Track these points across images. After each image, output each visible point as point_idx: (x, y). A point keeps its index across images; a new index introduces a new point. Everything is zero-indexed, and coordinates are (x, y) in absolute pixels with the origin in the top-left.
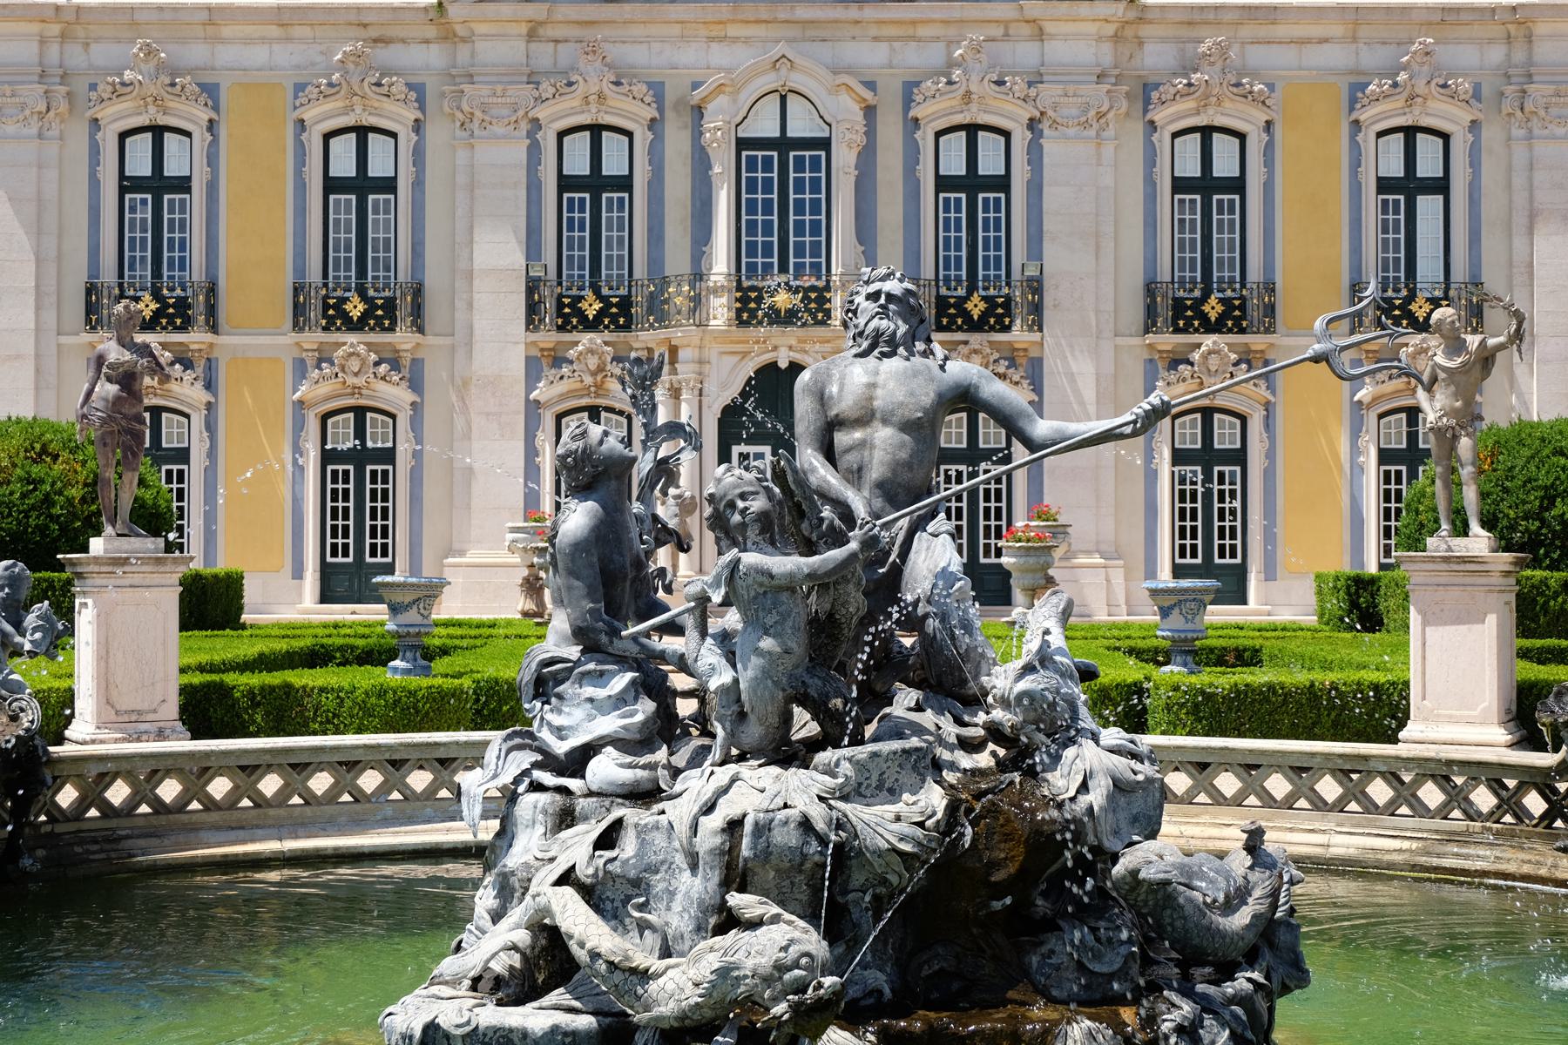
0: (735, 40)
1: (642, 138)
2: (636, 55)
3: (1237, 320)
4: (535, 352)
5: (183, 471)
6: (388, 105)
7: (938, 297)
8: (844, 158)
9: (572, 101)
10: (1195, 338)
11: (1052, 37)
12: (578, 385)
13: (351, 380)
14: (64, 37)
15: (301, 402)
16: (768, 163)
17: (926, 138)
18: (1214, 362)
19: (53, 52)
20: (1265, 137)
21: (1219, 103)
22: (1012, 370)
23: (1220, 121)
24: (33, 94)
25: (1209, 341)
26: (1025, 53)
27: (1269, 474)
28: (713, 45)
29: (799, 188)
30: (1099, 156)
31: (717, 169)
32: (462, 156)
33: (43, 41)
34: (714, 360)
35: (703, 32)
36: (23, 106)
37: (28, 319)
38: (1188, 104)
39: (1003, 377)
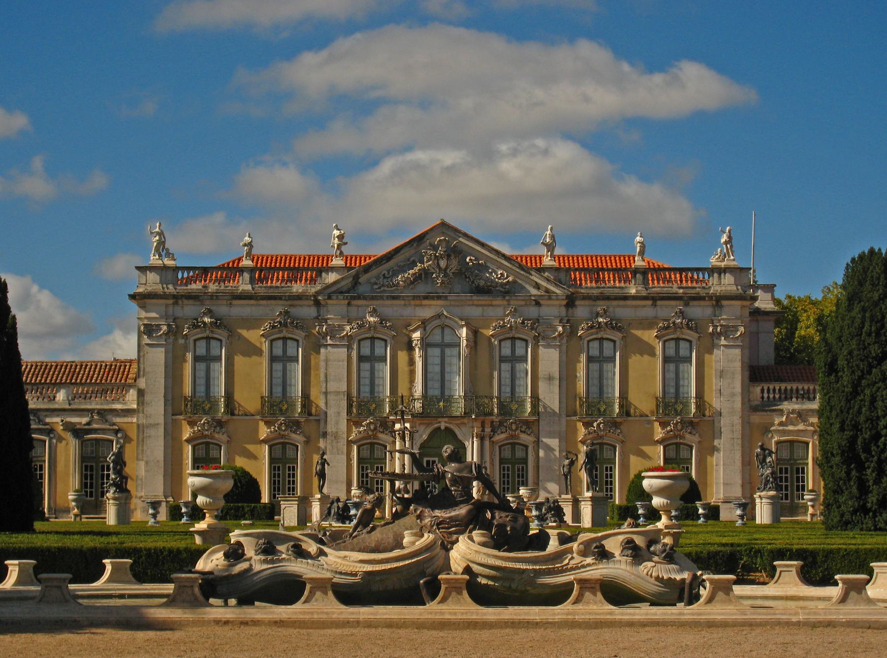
5: (42, 465)
12: (366, 435)
19: (170, 309)
21: (605, 330)
22: (527, 430)
23: (605, 336)
28: (417, 308)
33: (167, 306)
39: (524, 432)
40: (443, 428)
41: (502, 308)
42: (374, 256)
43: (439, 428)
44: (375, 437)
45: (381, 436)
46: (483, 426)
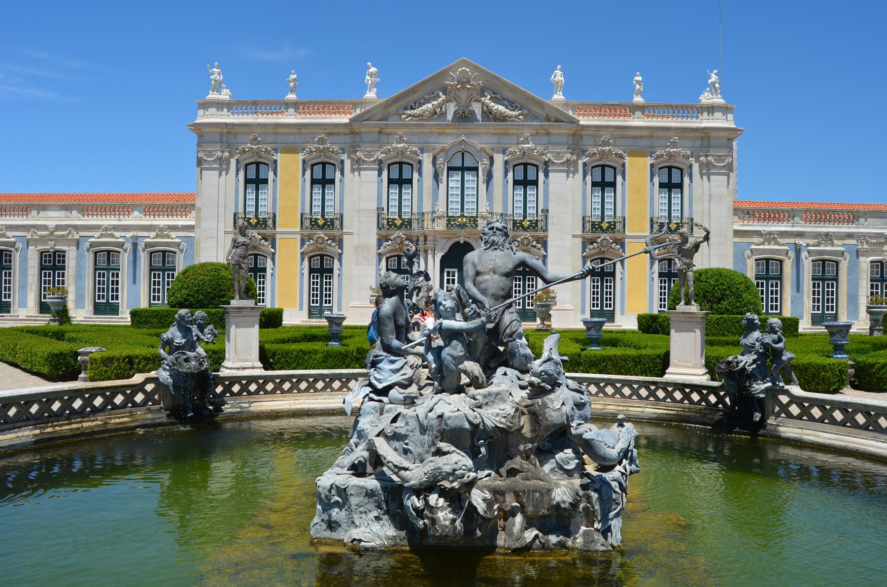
3: (613, 229)
11: (552, 134)
13: (319, 246)
18: (604, 243)
23: (607, 163)
25: (603, 236)
33: (221, 134)
34: (439, 240)
35: (436, 131)
39: (534, 247)
40: (462, 242)
44: (401, 249)
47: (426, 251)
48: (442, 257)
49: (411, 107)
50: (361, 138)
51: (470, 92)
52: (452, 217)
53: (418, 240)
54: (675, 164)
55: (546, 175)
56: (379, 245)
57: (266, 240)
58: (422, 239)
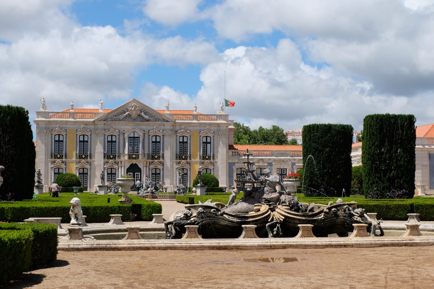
0: (128, 125)
1: (117, 137)
2: (117, 127)
4: (105, 162)
6: (87, 132)
7: (152, 155)
8: (141, 139)
9: (109, 132)
10: (181, 160)
14: (48, 124)
15: (77, 167)
16: (132, 139)
17: (151, 137)
18: (183, 163)
19: (47, 125)
20: (190, 137)
24: (45, 131)
25: (183, 161)
26: (162, 127)
27: (190, 176)
28: (126, 126)
29: (136, 143)
30: (171, 139)
31: (126, 140)
32: (96, 138)
33: (46, 124)
35: (125, 124)
36: (44, 132)
37: (44, 157)
38: (181, 133)
39: (159, 165)
40: (134, 164)
41: (152, 126)
42: (111, 110)
43: (133, 163)
44: (112, 166)
45: (114, 166)
46: (147, 163)
47: (121, 167)
48: (127, 169)
49: (116, 115)
50: (97, 126)
51: (137, 111)
52: (131, 155)
53: (118, 163)
54: (208, 136)
55: (163, 139)
56: (104, 164)
57: (63, 163)
58: (120, 162)
